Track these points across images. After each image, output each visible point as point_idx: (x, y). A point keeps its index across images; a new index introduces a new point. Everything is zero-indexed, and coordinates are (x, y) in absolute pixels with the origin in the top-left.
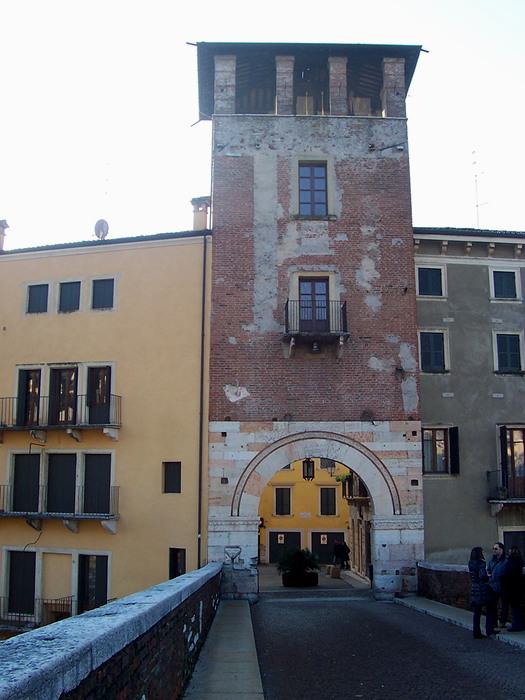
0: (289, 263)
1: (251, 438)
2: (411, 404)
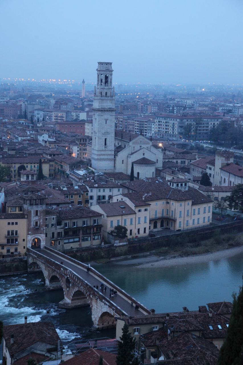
0: (35, 220)
1: (31, 236)
2: (45, 232)
